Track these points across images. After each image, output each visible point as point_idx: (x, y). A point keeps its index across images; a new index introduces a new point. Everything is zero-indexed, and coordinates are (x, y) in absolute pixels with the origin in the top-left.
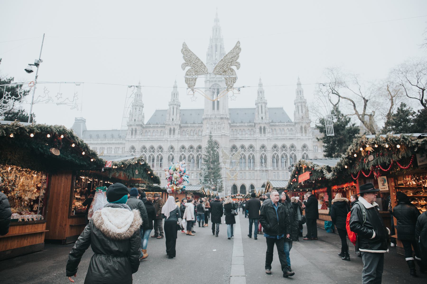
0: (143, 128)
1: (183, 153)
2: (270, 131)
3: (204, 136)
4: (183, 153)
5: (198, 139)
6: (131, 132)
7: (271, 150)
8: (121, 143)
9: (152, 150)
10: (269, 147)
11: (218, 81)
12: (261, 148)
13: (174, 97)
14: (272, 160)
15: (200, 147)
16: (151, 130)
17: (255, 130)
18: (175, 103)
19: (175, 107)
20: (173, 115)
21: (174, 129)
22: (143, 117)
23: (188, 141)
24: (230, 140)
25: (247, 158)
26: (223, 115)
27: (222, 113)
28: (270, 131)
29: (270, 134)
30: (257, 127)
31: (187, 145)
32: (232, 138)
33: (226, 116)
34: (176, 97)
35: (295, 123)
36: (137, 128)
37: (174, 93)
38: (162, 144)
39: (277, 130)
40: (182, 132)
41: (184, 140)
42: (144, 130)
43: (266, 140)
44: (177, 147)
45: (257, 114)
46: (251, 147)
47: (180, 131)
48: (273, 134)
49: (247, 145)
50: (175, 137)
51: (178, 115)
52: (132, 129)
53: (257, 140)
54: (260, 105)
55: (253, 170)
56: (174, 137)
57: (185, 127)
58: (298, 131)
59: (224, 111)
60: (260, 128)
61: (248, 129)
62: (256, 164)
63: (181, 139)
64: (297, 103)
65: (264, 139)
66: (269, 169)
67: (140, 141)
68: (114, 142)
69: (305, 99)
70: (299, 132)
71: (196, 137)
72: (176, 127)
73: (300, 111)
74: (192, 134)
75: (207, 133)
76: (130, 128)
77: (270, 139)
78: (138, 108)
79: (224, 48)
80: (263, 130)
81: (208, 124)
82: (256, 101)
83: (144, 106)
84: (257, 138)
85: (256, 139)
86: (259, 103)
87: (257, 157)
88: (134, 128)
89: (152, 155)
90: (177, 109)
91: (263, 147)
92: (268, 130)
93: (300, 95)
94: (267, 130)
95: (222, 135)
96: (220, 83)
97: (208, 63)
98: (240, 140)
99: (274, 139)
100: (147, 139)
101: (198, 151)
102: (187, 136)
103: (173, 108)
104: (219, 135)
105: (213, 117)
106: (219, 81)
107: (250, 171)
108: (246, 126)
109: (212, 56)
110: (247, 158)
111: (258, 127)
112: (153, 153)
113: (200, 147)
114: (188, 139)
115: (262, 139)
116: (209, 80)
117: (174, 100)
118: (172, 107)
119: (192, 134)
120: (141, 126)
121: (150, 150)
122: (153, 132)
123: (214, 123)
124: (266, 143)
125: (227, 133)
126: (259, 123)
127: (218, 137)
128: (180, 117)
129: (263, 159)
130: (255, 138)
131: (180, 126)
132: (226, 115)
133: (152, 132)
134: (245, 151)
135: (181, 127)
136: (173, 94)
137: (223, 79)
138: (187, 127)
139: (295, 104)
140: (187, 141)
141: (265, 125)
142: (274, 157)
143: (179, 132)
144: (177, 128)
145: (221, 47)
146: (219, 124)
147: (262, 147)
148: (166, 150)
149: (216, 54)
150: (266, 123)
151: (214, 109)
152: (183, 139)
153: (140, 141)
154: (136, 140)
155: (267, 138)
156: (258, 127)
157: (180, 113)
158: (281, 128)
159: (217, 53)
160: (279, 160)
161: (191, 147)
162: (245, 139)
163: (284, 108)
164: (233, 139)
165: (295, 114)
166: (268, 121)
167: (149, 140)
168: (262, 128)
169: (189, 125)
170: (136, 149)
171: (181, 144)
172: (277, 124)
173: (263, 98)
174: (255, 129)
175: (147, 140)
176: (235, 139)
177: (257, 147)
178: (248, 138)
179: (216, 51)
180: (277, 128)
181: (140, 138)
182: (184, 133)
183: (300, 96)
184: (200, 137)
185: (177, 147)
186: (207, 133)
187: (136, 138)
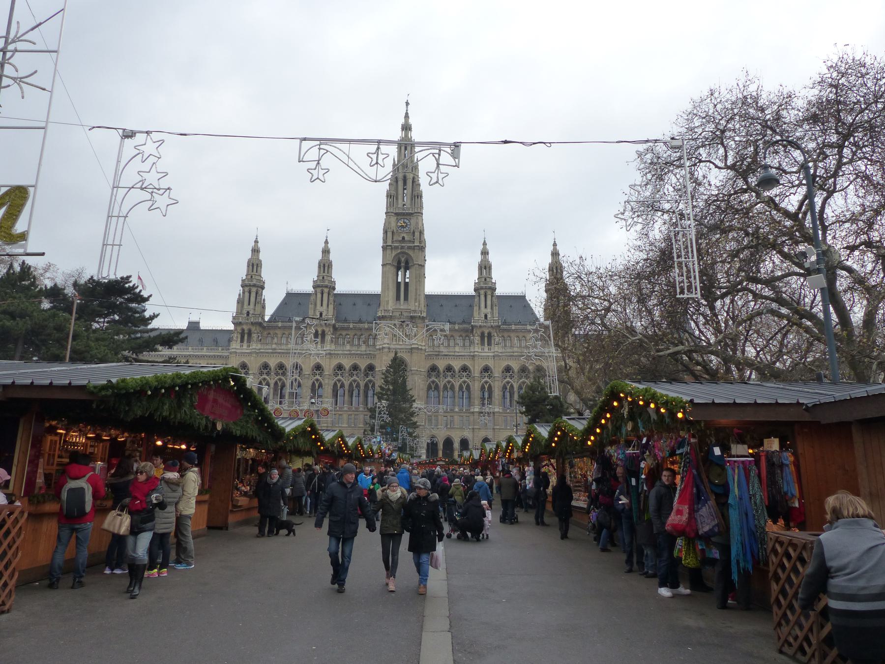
0: (264, 328)
1: (339, 377)
3: (379, 349)
4: (339, 377)
5: (368, 352)
6: (239, 336)
7: (500, 375)
8: (220, 357)
9: (280, 372)
10: (497, 371)
12: (482, 372)
13: (324, 272)
14: (502, 393)
15: (371, 368)
16: (279, 332)
17: (472, 338)
18: (326, 283)
19: (326, 290)
20: (322, 305)
21: (323, 332)
22: (264, 307)
23: (349, 356)
24: (426, 356)
25: (457, 389)
26: (415, 311)
27: (413, 308)
29: (500, 346)
30: (476, 332)
31: (347, 364)
32: (431, 351)
33: (421, 314)
36: (253, 329)
37: (324, 265)
38: (300, 361)
39: (513, 339)
40: (338, 338)
41: (342, 354)
42: (265, 333)
43: (492, 358)
44: (329, 366)
45: (476, 308)
46: (465, 369)
47: (334, 336)
48: (505, 346)
49: (457, 365)
50: (325, 349)
51: (331, 307)
52: (243, 330)
53: (476, 358)
54: (482, 292)
55: (468, 411)
56: (322, 347)
57: (343, 329)
59: (417, 304)
60: (482, 336)
61: (461, 336)
62: (472, 401)
63: (336, 352)
65: (489, 356)
66: (497, 410)
67: (258, 353)
68: (205, 352)
71: (363, 348)
72: (327, 330)
74: (356, 342)
75: (385, 344)
76: (239, 329)
77: (499, 356)
78: (254, 290)
80: (487, 339)
83: (266, 286)
84: (476, 353)
85: (473, 356)
86: (482, 288)
87: (476, 387)
88: (246, 328)
89: (280, 380)
90: (329, 294)
91: (486, 369)
92: (496, 338)
95: (412, 349)
97: (389, 212)
98: (445, 357)
99: (506, 356)
100: (271, 351)
101: (367, 375)
102: (348, 347)
103: (322, 294)
104: (407, 347)
105: (397, 314)
106: (409, 248)
107: (461, 413)
108: (456, 330)
109: (397, 199)
110: (457, 389)
111: (478, 332)
112: (282, 378)
113: (371, 368)
114: (348, 353)
115: (483, 356)
117: (323, 278)
118: (319, 290)
119: (356, 342)
120: (260, 324)
121: (277, 372)
122: (282, 337)
124: (490, 364)
125: (421, 345)
126: (480, 326)
127: (405, 351)
128: (334, 308)
129: (487, 393)
130: (472, 354)
131: (334, 326)
132: (421, 312)
133: (279, 336)
134: (454, 376)
135: (335, 328)
136: (322, 265)
137: (416, 244)
138: (348, 329)
140: (347, 356)
141: (490, 330)
142: (504, 388)
143: (332, 338)
144: (329, 331)
145: (413, 182)
147: (484, 369)
148: (308, 373)
149: (404, 193)
150: (492, 327)
151: (398, 298)
152: (341, 352)
153: (258, 353)
154: (250, 353)
155: (492, 354)
156: (478, 332)
157: (334, 302)
158: (521, 335)
159: (405, 191)
160: (514, 393)
161: (355, 367)
162: (453, 354)
164: (431, 355)
167: (274, 353)
168: (486, 335)
169: (351, 326)
170: (250, 368)
171: (335, 362)
172: (513, 327)
173: (488, 280)
175: (272, 353)
176: (436, 355)
177: (476, 371)
178: (458, 352)
179: (404, 189)
180: (512, 335)
181: (257, 348)
182: (341, 341)
184: (371, 348)
185: (329, 366)
186: (385, 344)
187: (250, 348)
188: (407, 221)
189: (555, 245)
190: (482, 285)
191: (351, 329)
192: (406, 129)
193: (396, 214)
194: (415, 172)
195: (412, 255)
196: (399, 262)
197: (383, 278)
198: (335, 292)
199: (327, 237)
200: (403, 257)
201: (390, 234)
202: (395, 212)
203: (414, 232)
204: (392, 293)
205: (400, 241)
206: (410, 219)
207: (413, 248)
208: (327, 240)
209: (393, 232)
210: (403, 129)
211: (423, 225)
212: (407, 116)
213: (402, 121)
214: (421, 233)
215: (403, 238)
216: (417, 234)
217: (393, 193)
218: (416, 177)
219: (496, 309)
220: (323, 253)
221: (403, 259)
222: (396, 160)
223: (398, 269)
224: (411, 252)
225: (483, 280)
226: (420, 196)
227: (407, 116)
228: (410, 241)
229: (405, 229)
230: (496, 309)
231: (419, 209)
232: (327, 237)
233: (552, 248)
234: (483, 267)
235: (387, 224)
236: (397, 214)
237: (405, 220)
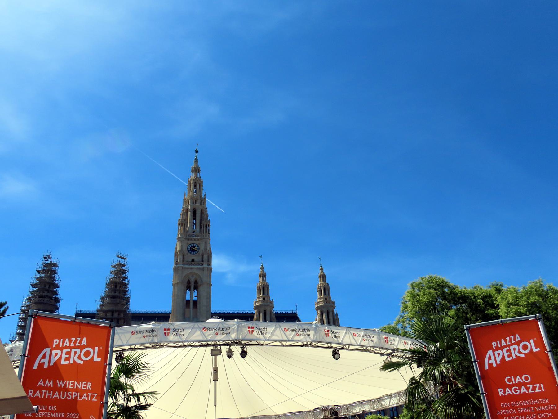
79: (207, 215)
192: (196, 171)
194: (204, 205)
196: (189, 282)
200: (193, 276)
216: (205, 257)
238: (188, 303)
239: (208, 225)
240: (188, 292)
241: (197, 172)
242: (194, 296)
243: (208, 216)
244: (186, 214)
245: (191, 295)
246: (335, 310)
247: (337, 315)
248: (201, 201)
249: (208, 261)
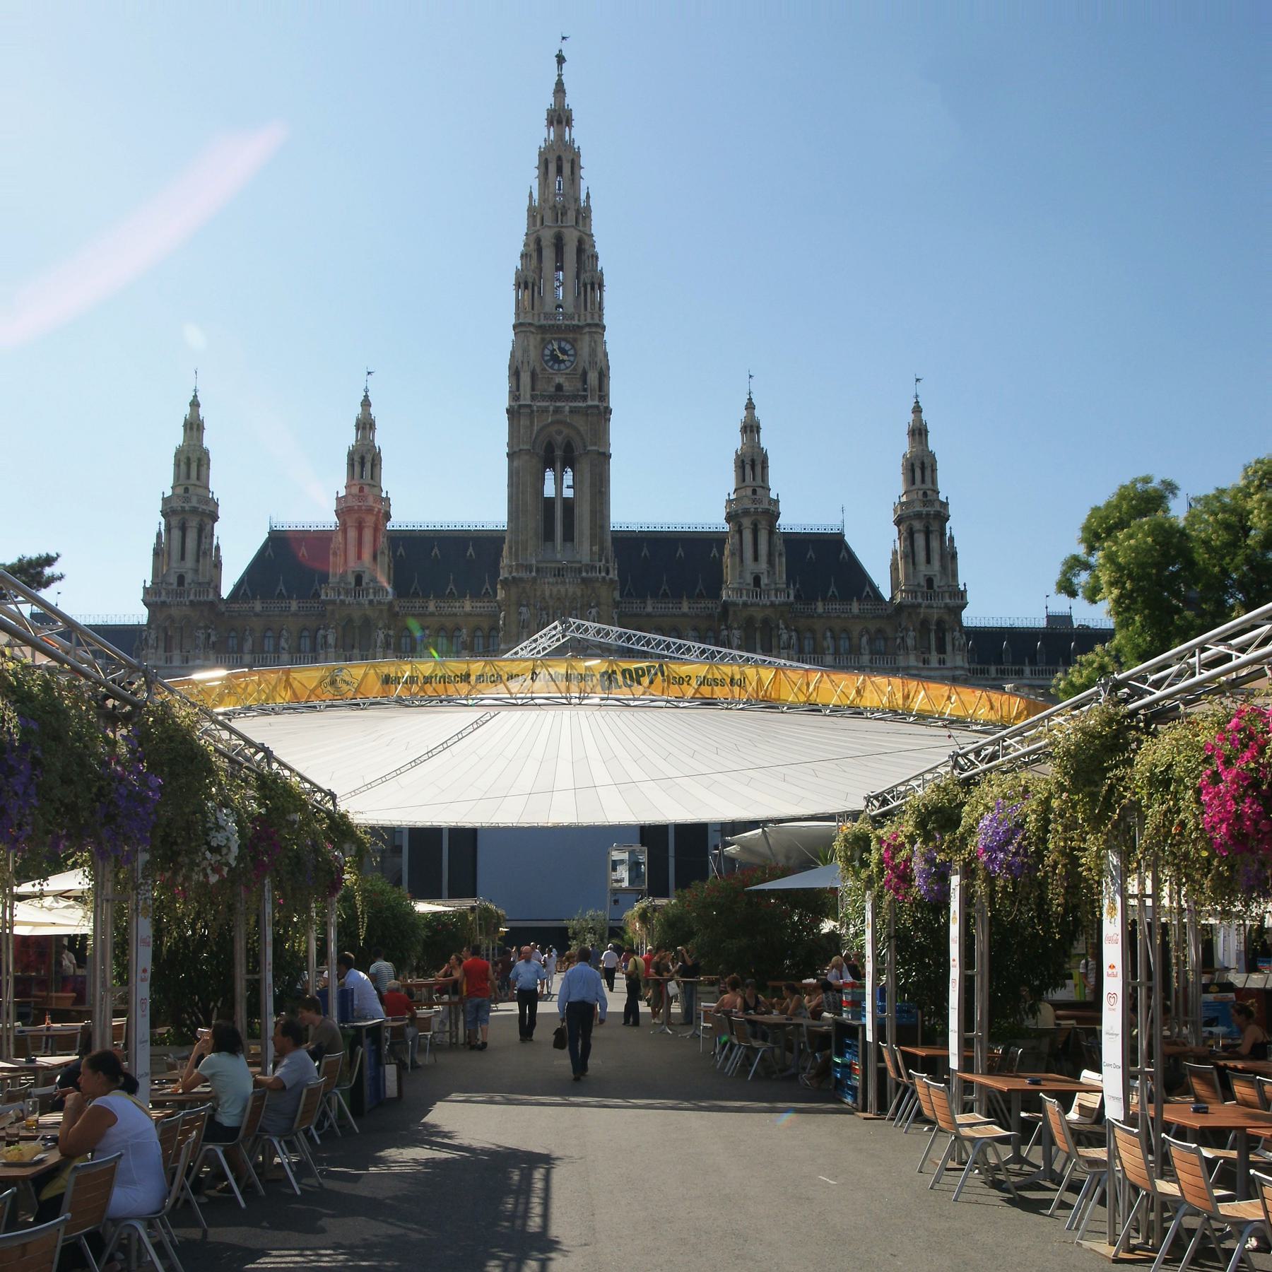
2: (790, 637)
11: (567, 409)
17: (725, 633)
18: (370, 502)
26: (593, 568)
27: (586, 559)
28: (790, 637)
29: (791, 652)
33: (608, 573)
34: (372, 478)
35: (900, 607)
37: (362, 459)
47: (391, 633)
54: (746, 522)
58: (910, 642)
59: (596, 548)
64: (909, 517)
69: (942, 503)
70: (915, 649)
73: (921, 556)
79: (595, 257)
81: (527, 606)
82: (729, 501)
86: (746, 512)
90: (376, 529)
93: (923, 481)
94: (779, 636)
96: (579, 422)
103: (360, 529)
108: (684, 615)
116: (530, 406)
123: (551, 603)
126: (745, 604)
136: (357, 458)
137: (590, 403)
139: (898, 522)
143: (387, 636)
145: (580, 250)
146: (576, 609)
150: (772, 605)
151: (548, 535)
163: (848, 539)
165: (894, 568)
166: (782, 598)
173: (759, 491)
174: (729, 628)
183: (924, 487)
188: (568, 347)
189: (917, 410)
190: (748, 504)
191: (432, 614)
192: (560, 122)
193: (540, 327)
194: (585, 225)
195: (582, 429)
196: (550, 448)
197: (510, 485)
198: (389, 526)
199: (366, 391)
200: (560, 433)
201: (525, 378)
202: (536, 322)
203: (585, 374)
204: (534, 522)
205: (552, 398)
206: (575, 340)
207: (585, 412)
208: (366, 396)
209: (533, 375)
210: (550, 122)
211: (606, 355)
212: (560, 89)
213: (549, 100)
214: (603, 375)
215: (559, 387)
216: (593, 377)
217: (531, 276)
218: (586, 238)
219: (781, 564)
220: (358, 430)
221: (559, 439)
222: (536, 195)
223: (549, 463)
224: (579, 422)
225: (749, 491)
226: (597, 284)
227: (560, 89)
228: (574, 397)
229: (562, 366)
230: (780, 562)
231: (596, 316)
232: (366, 391)
233: (910, 417)
234: (748, 461)
235: (519, 354)
236: (542, 329)
237: (563, 344)
238: (549, 502)
239: (596, 286)
240: (549, 475)
241: (564, 123)
242: (565, 485)
243: (597, 258)
244: (535, 255)
245: (559, 482)
246: (948, 525)
247: (952, 539)
248: (578, 212)
249: (600, 390)
